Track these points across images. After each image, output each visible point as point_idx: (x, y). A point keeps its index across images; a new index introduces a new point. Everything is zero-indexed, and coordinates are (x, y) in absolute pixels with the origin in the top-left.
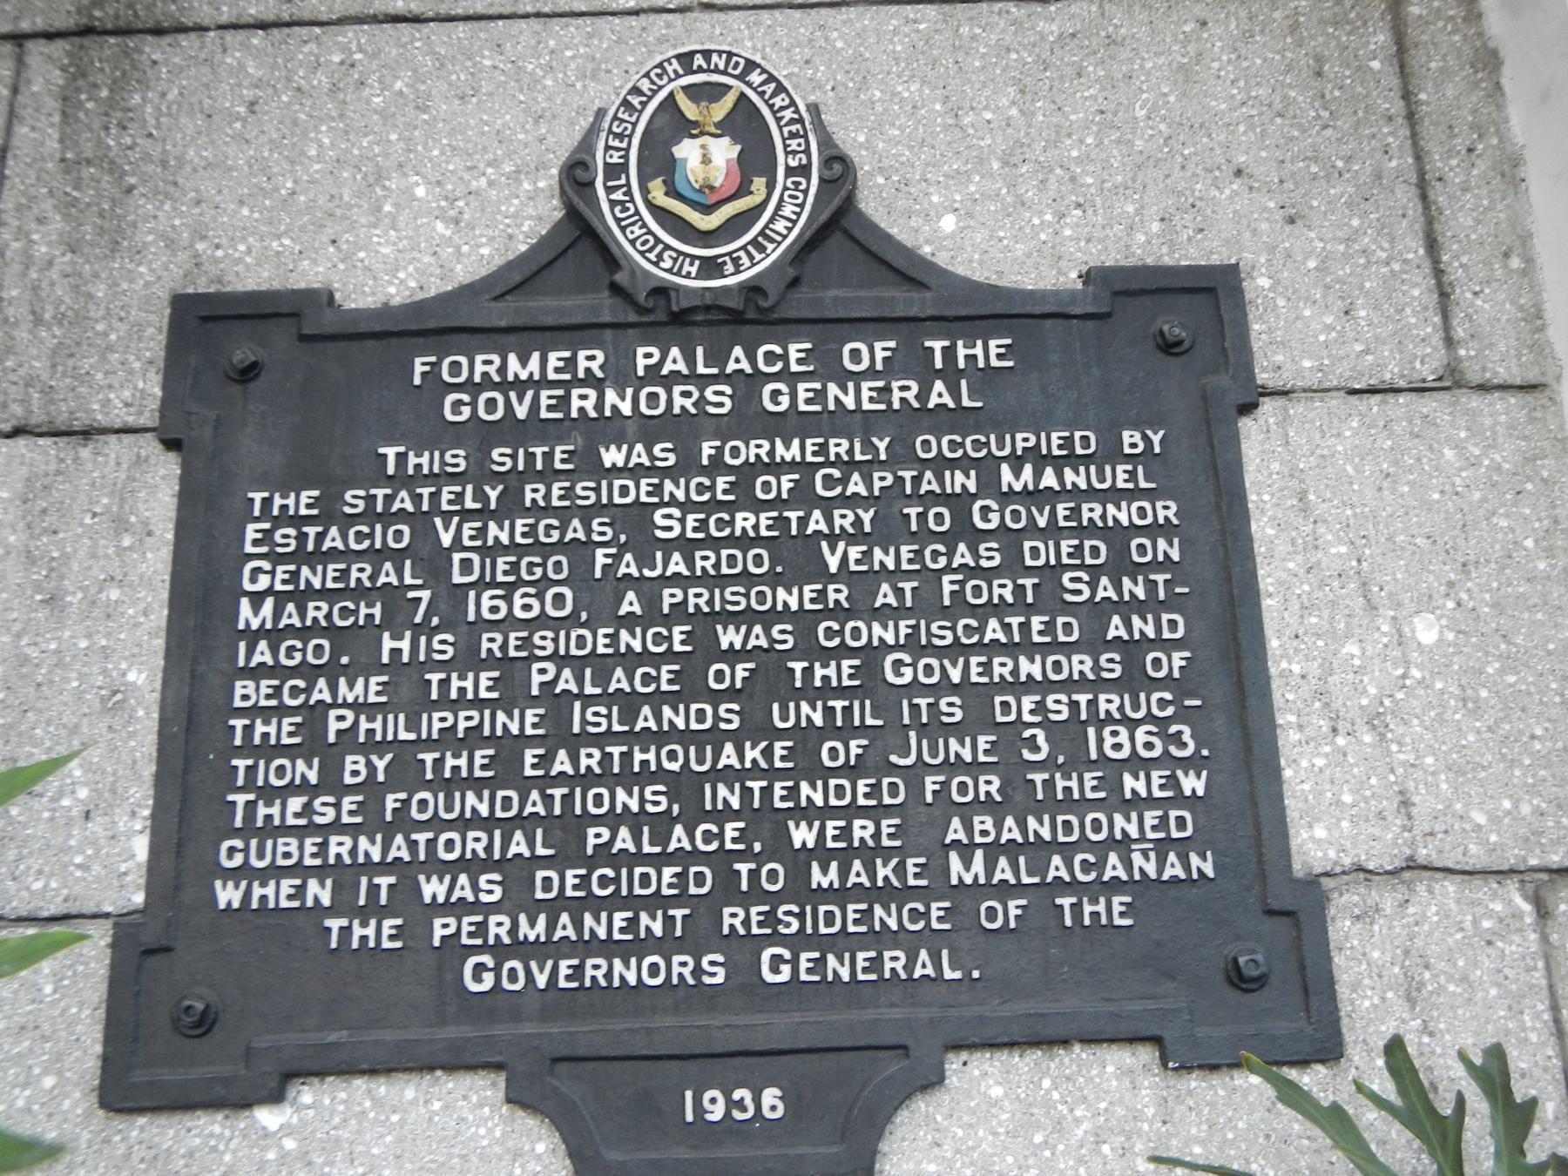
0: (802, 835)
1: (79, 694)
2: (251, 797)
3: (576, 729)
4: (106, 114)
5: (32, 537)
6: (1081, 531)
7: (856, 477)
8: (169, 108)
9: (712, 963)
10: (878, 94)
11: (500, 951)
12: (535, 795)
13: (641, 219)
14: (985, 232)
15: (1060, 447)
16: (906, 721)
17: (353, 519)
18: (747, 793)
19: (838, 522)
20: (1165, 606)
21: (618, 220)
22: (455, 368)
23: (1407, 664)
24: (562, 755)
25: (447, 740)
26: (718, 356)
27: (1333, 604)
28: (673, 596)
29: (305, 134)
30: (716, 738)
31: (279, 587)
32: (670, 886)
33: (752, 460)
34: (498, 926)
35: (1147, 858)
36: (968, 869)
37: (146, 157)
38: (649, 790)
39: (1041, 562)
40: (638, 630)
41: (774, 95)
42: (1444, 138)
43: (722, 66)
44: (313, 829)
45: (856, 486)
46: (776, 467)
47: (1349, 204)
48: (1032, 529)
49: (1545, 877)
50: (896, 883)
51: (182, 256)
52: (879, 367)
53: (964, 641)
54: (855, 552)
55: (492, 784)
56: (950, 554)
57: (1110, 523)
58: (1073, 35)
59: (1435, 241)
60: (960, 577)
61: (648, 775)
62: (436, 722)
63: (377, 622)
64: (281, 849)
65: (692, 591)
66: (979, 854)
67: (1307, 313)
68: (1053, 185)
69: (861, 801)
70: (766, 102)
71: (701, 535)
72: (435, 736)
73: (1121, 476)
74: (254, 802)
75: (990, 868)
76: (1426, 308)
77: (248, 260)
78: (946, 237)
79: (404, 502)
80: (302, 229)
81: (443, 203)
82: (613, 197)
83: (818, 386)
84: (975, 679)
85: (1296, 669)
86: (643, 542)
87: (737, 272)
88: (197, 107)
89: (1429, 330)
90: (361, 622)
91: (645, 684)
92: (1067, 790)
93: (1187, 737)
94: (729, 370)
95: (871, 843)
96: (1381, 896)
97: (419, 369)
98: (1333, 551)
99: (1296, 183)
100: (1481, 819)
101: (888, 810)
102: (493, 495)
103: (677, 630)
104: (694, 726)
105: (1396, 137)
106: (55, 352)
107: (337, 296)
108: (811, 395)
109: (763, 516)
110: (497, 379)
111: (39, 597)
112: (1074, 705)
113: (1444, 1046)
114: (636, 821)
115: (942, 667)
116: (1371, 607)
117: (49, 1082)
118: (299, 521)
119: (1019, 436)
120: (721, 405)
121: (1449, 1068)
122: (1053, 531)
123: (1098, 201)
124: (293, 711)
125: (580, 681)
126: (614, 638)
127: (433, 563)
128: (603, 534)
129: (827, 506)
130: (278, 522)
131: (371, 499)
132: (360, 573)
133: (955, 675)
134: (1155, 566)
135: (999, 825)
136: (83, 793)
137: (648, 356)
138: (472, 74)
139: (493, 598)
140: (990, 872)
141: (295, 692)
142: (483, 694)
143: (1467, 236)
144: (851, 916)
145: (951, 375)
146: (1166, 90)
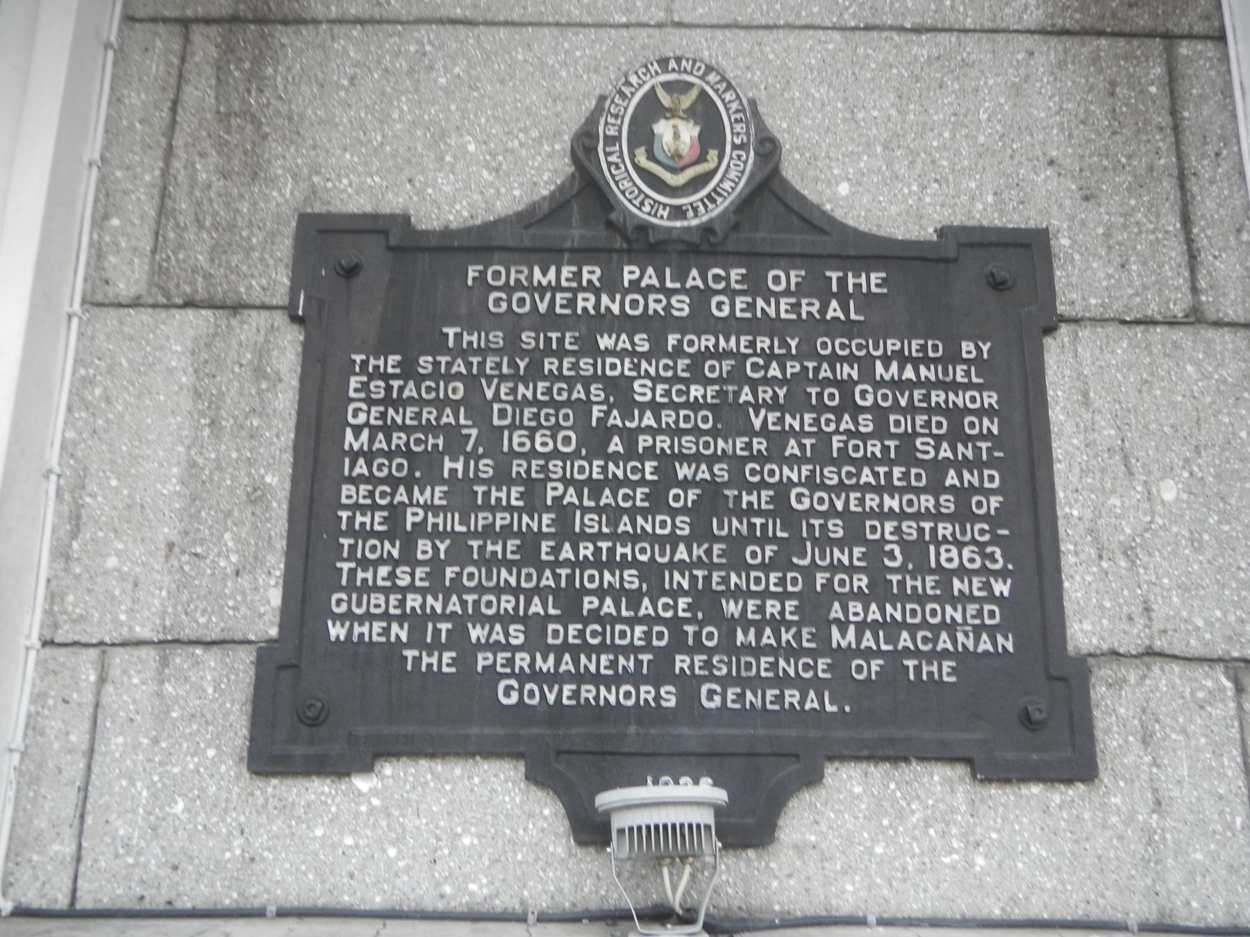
0: (732, 608)
1: (231, 490)
2: (353, 565)
3: (577, 529)
5: (198, 378)
6: (929, 411)
7: (774, 364)
8: (293, 78)
9: (667, 693)
10: (797, 94)
11: (522, 678)
12: (548, 573)
14: (870, 197)
15: (917, 351)
16: (805, 535)
17: (425, 377)
18: (694, 579)
19: (761, 395)
20: (988, 465)
23: (1153, 513)
24: (567, 546)
25: (488, 532)
26: (681, 276)
27: (1103, 470)
29: (390, 102)
30: (673, 540)
31: (373, 422)
32: (640, 639)
33: (703, 349)
34: (522, 660)
37: (277, 113)
39: (902, 430)
40: (621, 464)
41: (725, 91)
42: (1199, 144)
43: (689, 69)
44: (395, 588)
45: (774, 371)
46: (720, 355)
47: (1129, 189)
48: (896, 407)
49: (1242, 665)
50: (794, 645)
51: (303, 186)
52: (793, 288)
53: (846, 482)
54: (772, 417)
55: (519, 565)
56: (838, 423)
57: (951, 405)
58: (938, 58)
59: (1189, 218)
60: (844, 438)
61: (625, 564)
62: (481, 520)
63: (441, 448)
64: (373, 601)
65: (659, 438)
66: (852, 629)
67: (1095, 265)
68: (919, 166)
69: (772, 588)
70: (720, 97)
72: (480, 529)
73: (959, 373)
75: (859, 638)
76: (1180, 266)
78: (842, 199)
79: (459, 367)
80: (389, 170)
84: (853, 508)
85: (1075, 513)
86: (627, 405)
88: (313, 80)
89: (1181, 281)
90: (429, 448)
92: (914, 588)
93: (998, 555)
94: (688, 285)
95: (778, 617)
96: (1128, 671)
97: (471, 274)
98: (1105, 433)
99: (1092, 173)
100: (1200, 623)
101: (791, 596)
102: (522, 365)
104: (658, 531)
105: (1163, 143)
106: (213, 249)
107: (413, 219)
109: (709, 389)
112: (921, 531)
113: (1167, 775)
114: (617, 593)
115: (830, 498)
116: (1130, 473)
117: (211, 753)
118: (386, 377)
120: (682, 310)
121: (1169, 790)
122: (911, 409)
123: (951, 179)
124: (382, 508)
125: (580, 497)
126: (604, 469)
129: (754, 385)
130: (371, 377)
131: (436, 364)
132: (429, 414)
133: (839, 505)
134: (981, 437)
137: (631, 272)
139: (521, 436)
140: (859, 641)
141: (383, 495)
142: (514, 503)
143: (1212, 216)
144: (763, 665)
146: (1002, 101)
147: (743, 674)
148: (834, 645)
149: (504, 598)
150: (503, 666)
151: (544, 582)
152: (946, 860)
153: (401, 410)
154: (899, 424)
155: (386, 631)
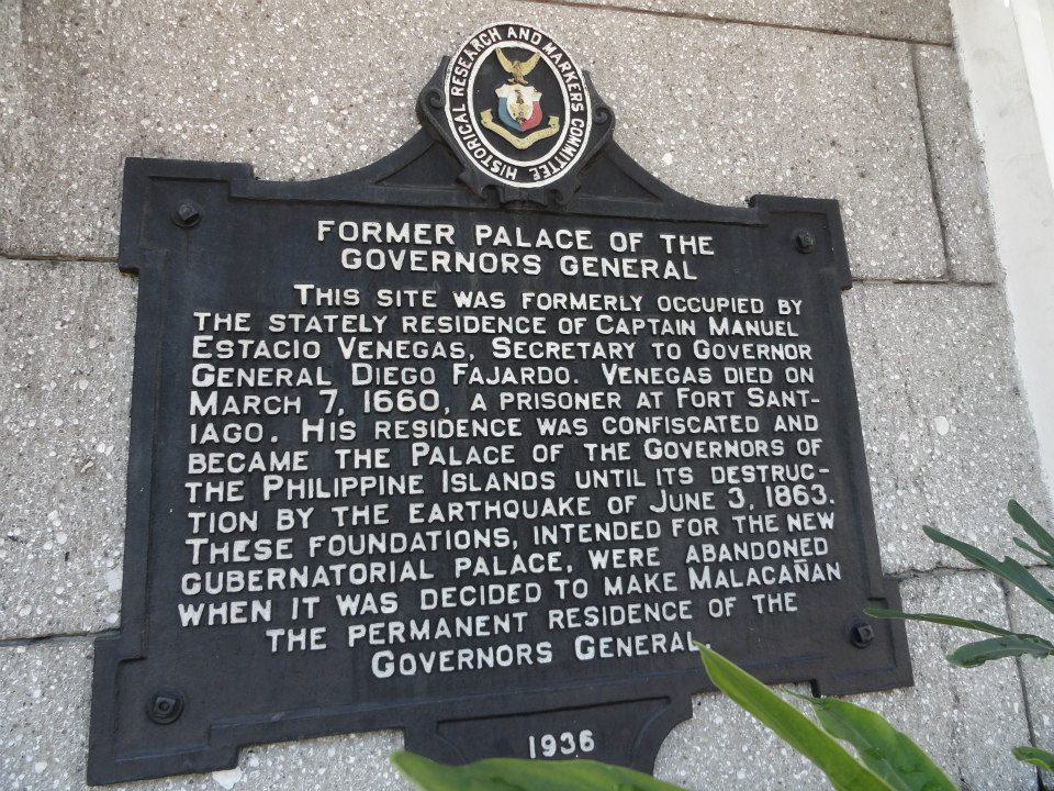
1: (56, 462)
2: (205, 541)
3: (445, 490)
4: (61, 11)
5: (9, 337)
7: (622, 321)
8: (114, 14)
9: (543, 649)
11: (398, 648)
12: (418, 536)
13: (477, 137)
15: (743, 308)
16: (659, 483)
17: (277, 336)
18: (561, 533)
19: (612, 351)
21: (461, 136)
22: (349, 231)
23: (933, 446)
24: (436, 508)
25: (354, 498)
26: (531, 235)
28: (507, 398)
29: (225, 48)
30: (540, 495)
31: (221, 384)
32: (513, 597)
33: (556, 307)
34: (396, 630)
35: (803, 568)
36: (700, 579)
37: (96, 49)
38: (496, 531)
40: (485, 421)
41: (561, 62)
43: (527, 38)
45: (622, 328)
46: (573, 313)
48: (729, 360)
50: (658, 590)
52: (633, 250)
53: (692, 431)
54: (623, 372)
55: (388, 529)
56: (682, 374)
58: (738, 46)
60: (687, 390)
61: (495, 522)
62: (346, 484)
63: (298, 412)
64: (230, 580)
65: (519, 395)
66: (707, 569)
69: (634, 537)
70: (556, 66)
71: (524, 357)
72: (344, 495)
73: (779, 328)
74: (208, 545)
75: (714, 578)
77: (184, 136)
78: (666, 168)
79: (314, 325)
81: (332, 111)
82: (457, 119)
83: (595, 259)
84: (699, 455)
86: (487, 363)
87: (542, 179)
88: (137, 17)
90: (286, 412)
91: (491, 458)
93: (822, 492)
94: (538, 245)
95: (641, 564)
97: (322, 230)
101: (650, 543)
102: (380, 323)
103: (511, 421)
104: (525, 487)
106: (24, 193)
107: (255, 170)
108: (592, 265)
109: (564, 345)
110: (379, 240)
111: (18, 386)
112: (758, 473)
114: (488, 553)
116: (914, 413)
117: (40, 767)
118: (234, 336)
119: (719, 300)
120: (534, 268)
121: (964, 687)
122: (741, 362)
124: (236, 477)
125: (446, 457)
126: (469, 427)
127: (338, 370)
128: (458, 353)
129: (605, 340)
130: (218, 336)
131: (290, 322)
132: (283, 375)
133: (688, 453)
134: (800, 385)
135: (718, 550)
136: (62, 539)
137: (484, 231)
138: (349, 20)
139: (382, 396)
140: (714, 580)
141: (236, 462)
142: (379, 465)
143: (954, 193)
144: (631, 613)
145: (677, 258)
146: (791, 87)
147: (614, 623)
148: (693, 587)
149: (373, 565)
150: (376, 637)
151: (414, 546)
152: (798, 777)
153: (252, 371)
154: (733, 375)
155: (247, 611)
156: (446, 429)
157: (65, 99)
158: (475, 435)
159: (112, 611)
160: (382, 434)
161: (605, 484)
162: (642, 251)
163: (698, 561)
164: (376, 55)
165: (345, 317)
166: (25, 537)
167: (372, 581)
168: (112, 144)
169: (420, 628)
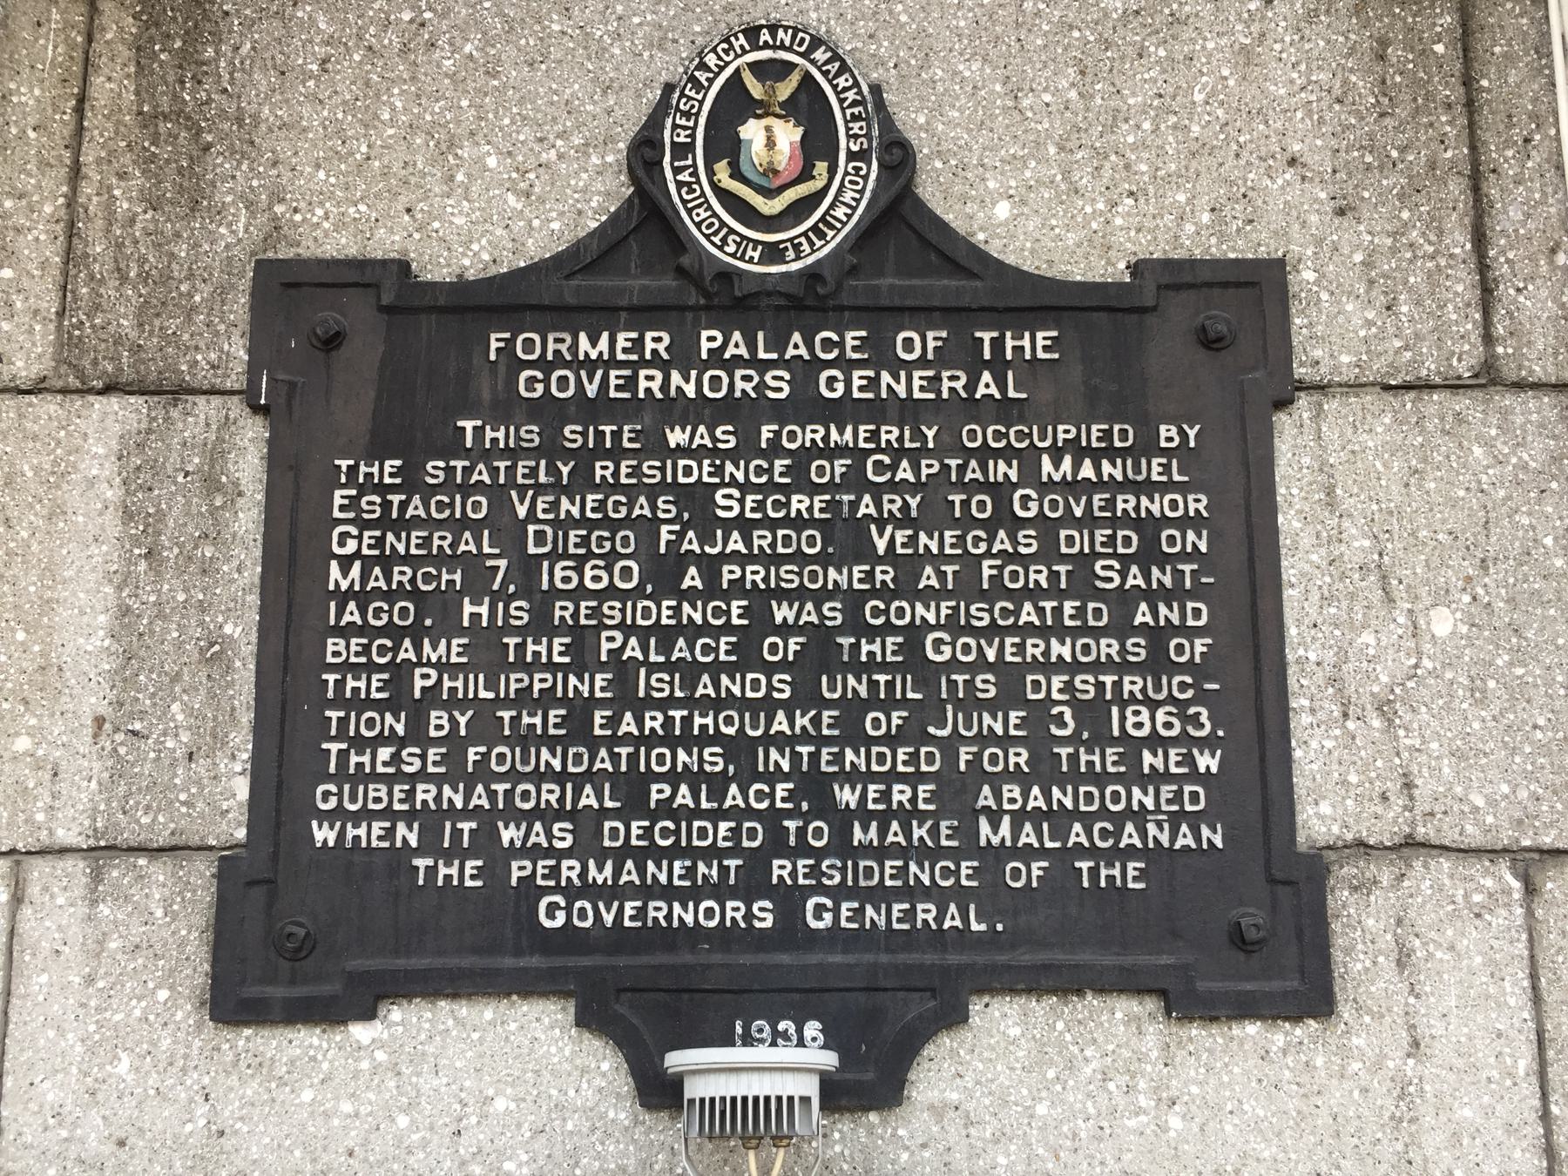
0: (847, 796)
1: (179, 645)
2: (344, 746)
3: (641, 694)
4: (180, 67)
5: (127, 492)
6: (1114, 523)
7: (905, 464)
8: (242, 63)
9: (761, 909)
10: (939, 72)
11: (572, 893)
12: (603, 753)
13: (707, 201)
14: (1038, 221)
15: (1099, 439)
16: (944, 696)
19: (886, 506)
20: (1193, 594)
21: (684, 202)
22: (529, 345)
23: (1420, 654)
24: (628, 716)
26: (778, 342)
27: (1352, 596)
28: (731, 572)
29: (378, 96)
30: (769, 705)
31: (365, 551)
32: (725, 839)
33: (808, 444)
34: (570, 870)
35: (1161, 829)
36: (995, 833)
38: (707, 751)
39: (1076, 550)
41: (838, 74)
42: (1502, 127)
43: (787, 43)
44: (399, 776)
45: (905, 473)
46: (832, 452)
47: (1401, 197)
48: (1069, 519)
49: (1536, 856)
50: (930, 844)
51: (262, 219)
52: (930, 356)
53: (1000, 622)
56: (991, 541)
57: (1143, 515)
58: (1137, 12)
59: (1484, 235)
60: (999, 562)
61: (705, 739)
62: (514, 682)
64: (372, 794)
65: (749, 569)
66: (1006, 819)
67: (1349, 307)
68: (1107, 173)
69: (901, 768)
70: (830, 82)
71: (758, 516)
72: (512, 696)
73: (1156, 469)
74: (348, 751)
76: (1468, 305)
77: (326, 225)
78: (1000, 225)
79: (482, 475)
80: (377, 196)
81: (514, 175)
82: (679, 178)
83: (871, 373)
84: (1009, 658)
85: (1312, 656)
86: (707, 523)
87: (798, 258)
89: (1469, 326)
91: (704, 654)
92: (1090, 764)
93: (1204, 718)
95: (908, 806)
96: (1379, 870)
98: (1357, 544)
99: (1349, 174)
100: (1480, 802)
102: (565, 470)
103: (735, 604)
104: (749, 694)
105: (1450, 126)
108: (864, 382)
109: (817, 499)
110: (568, 358)
111: (137, 551)
112: (1100, 686)
113: (1428, 1007)
114: (695, 778)
115: (979, 646)
116: (1390, 599)
117: (163, 994)
118: (383, 490)
119: (1061, 428)
120: (780, 390)
122: (1089, 522)
123: (1151, 190)
124: (381, 668)
126: (677, 611)
127: (509, 533)
128: (668, 511)
129: (877, 491)
131: (450, 471)
133: (991, 655)
134: (1184, 556)
135: (1026, 795)
136: (185, 737)
137: (711, 339)
138: (541, 39)
139: (564, 568)
140: (1015, 838)
141: (382, 650)
142: (557, 659)
143: (1516, 231)
144: (888, 871)
145: (999, 366)
146: (1226, 72)
147: (862, 883)
148: (983, 843)
149: (545, 787)
150: (544, 877)
151: (598, 765)
152: (1132, 1123)
153: (404, 535)
154: (1072, 541)
155: (390, 833)
156: (646, 612)
157: (185, 184)
158: (685, 622)
159: (239, 825)
160: (562, 618)
161: (864, 693)
162: (943, 358)
163: (994, 807)
164: (576, 86)
165: (520, 464)
166: (146, 732)
167: (543, 806)
168: (240, 240)
169: (600, 870)
